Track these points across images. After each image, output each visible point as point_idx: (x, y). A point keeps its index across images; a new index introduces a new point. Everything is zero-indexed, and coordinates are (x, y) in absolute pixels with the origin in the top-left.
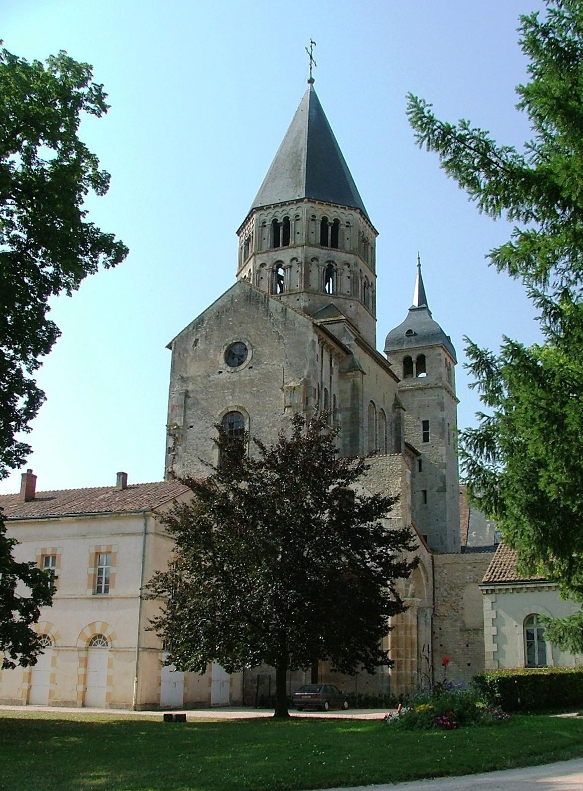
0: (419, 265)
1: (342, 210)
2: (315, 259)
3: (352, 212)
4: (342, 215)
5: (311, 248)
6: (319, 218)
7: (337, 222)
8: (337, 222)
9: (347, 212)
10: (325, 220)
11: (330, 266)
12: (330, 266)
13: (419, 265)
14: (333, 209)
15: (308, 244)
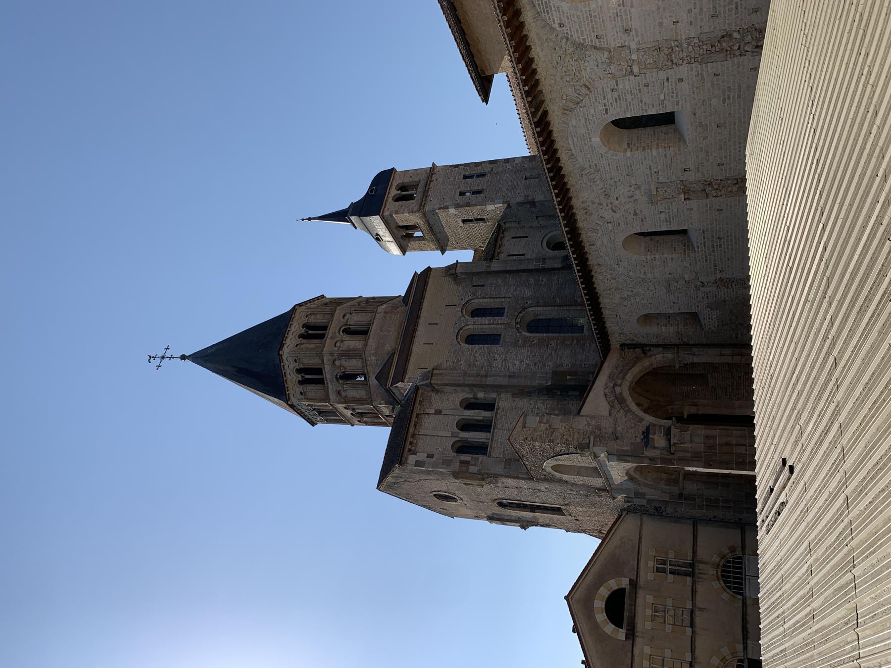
0: (309, 219)
1: (286, 367)
2: (339, 393)
3: (284, 357)
4: (291, 367)
5: (331, 397)
6: (300, 389)
7: (299, 371)
8: (299, 371)
9: (287, 363)
10: (301, 383)
11: (342, 378)
12: (342, 378)
13: (309, 219)
14: (288, 376)
15: (326, 399)
